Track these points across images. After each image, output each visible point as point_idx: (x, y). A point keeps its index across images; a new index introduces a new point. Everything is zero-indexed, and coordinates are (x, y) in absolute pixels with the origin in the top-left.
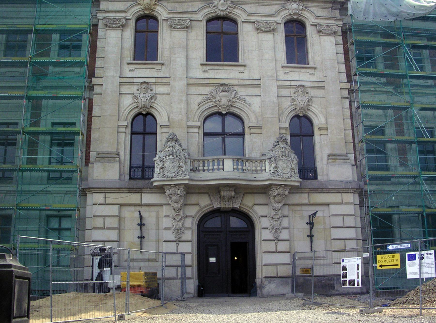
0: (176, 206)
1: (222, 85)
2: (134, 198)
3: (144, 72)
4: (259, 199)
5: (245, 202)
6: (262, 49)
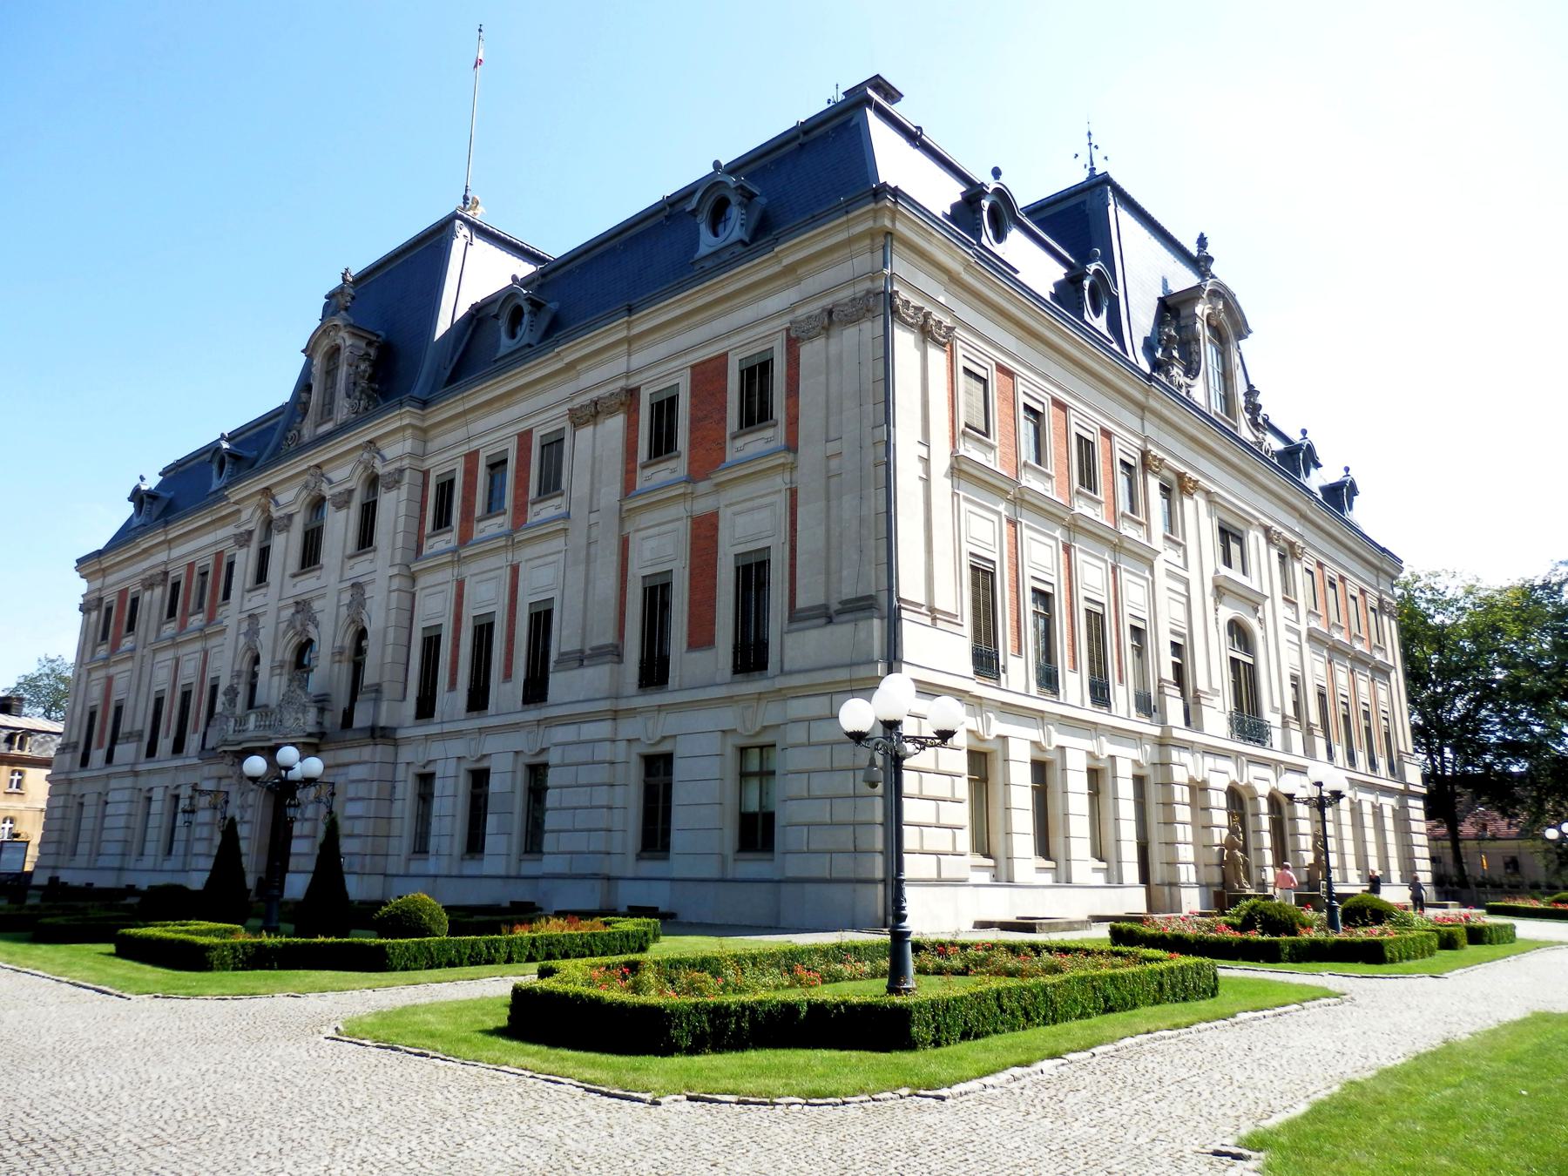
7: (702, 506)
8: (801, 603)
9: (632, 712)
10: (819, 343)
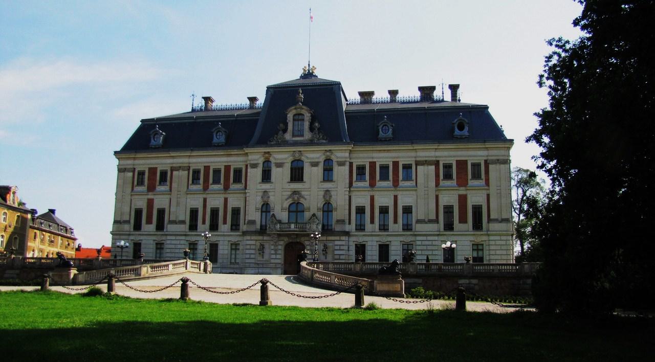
0: (275, 241)
1: (295, 191)
2: (261, 238)
3: (266, 186)
4: (306, 238)
5: (301, 239)
6: (313, 174)
7: (150, 197)
8: (171, 219)
9: (133, 235)
10: (177, 172)
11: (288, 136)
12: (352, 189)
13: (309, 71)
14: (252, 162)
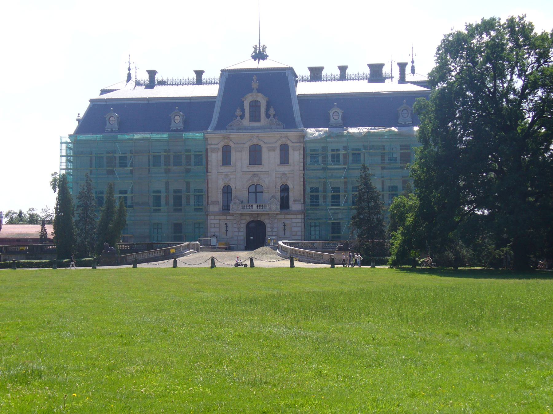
1: (254, 174)
2: (224, 217)
3: (226, 169)
6: (270, 158)
11: (246, 122)
12: (307, 172)
13: (260, 50)
14: (213, 146)
